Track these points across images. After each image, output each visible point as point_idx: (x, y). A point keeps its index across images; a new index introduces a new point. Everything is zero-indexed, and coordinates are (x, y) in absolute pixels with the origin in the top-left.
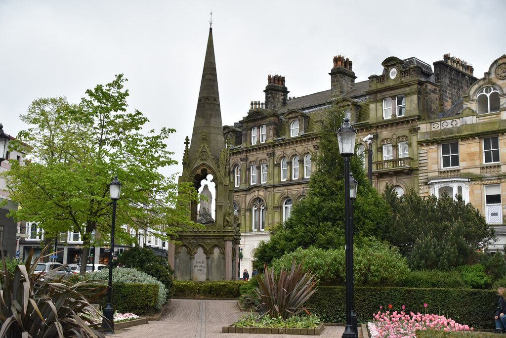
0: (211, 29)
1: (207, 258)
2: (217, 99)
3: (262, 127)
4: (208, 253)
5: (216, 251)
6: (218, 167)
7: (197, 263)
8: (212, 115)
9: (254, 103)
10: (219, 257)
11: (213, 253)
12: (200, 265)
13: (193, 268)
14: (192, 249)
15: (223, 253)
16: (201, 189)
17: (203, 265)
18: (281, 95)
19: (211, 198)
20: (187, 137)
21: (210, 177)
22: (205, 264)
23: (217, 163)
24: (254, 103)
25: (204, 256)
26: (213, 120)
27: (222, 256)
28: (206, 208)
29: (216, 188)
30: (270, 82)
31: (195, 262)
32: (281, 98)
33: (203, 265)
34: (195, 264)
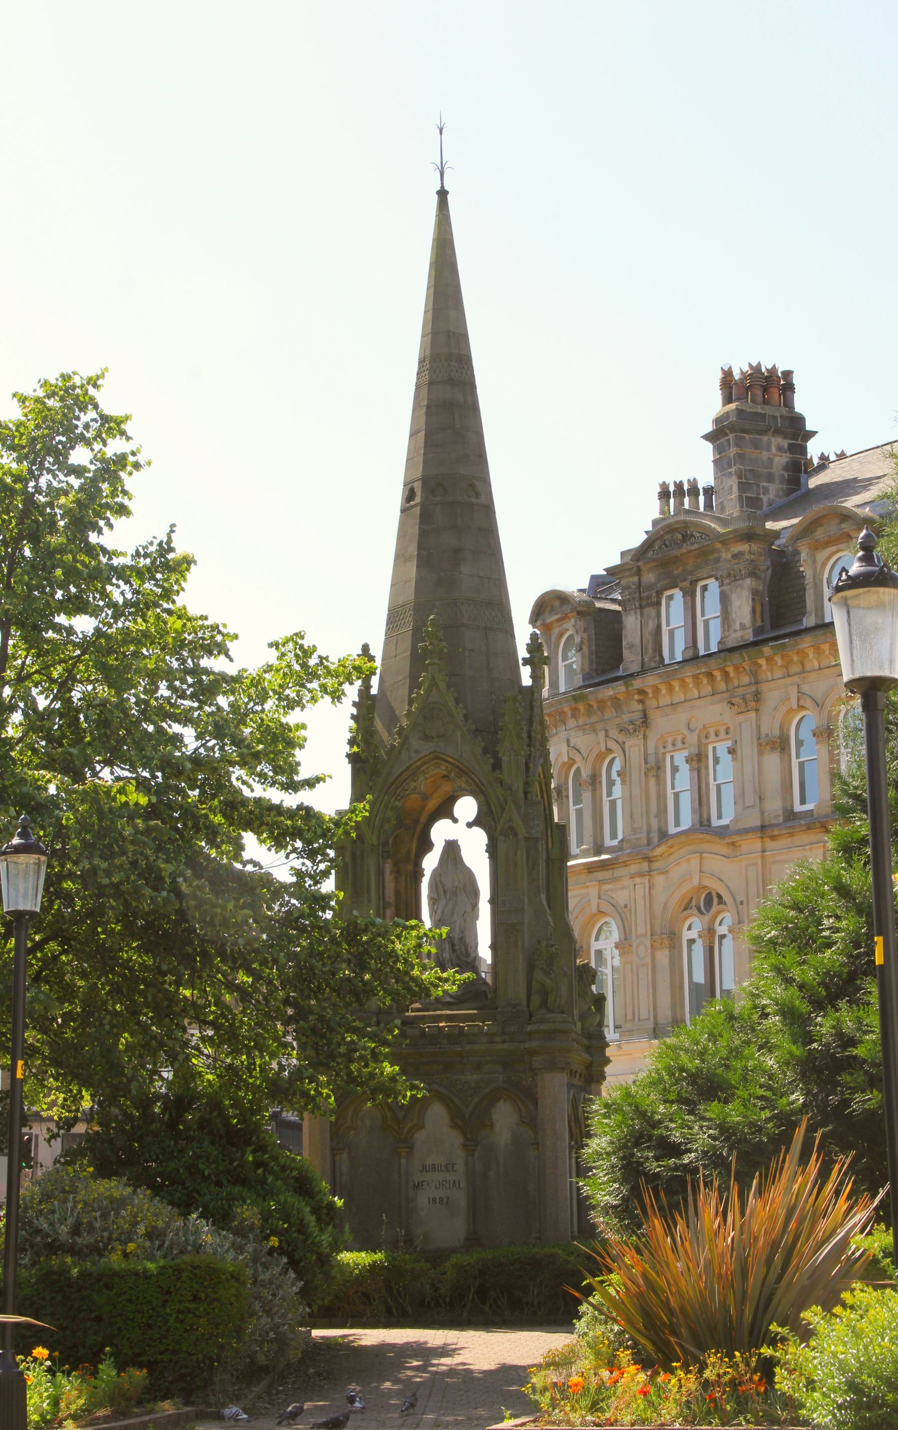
0: (443, 194)
1: (469, 1145)
2: (479, 486)
3: (705, 588)
4: (471, 1124)
5: (504, 1118)
6: (497, 766)
7: (424, 1169)
8: (457, 551)
9: (672, 488)
11: (492, 1126)
15: (531, 1120)
16: (430, 862)
17: (450, 1177)
18: (780, 449)
19: (476, 893)
20: (366, 648)
21: (467, 807)
23: (491, 750)
24: (672, 488)
25: (455, 1139)
26: (466, 569)
29: (492, 849)
30: (728, 400)
32: (781, 460)
33: (450, 1177)
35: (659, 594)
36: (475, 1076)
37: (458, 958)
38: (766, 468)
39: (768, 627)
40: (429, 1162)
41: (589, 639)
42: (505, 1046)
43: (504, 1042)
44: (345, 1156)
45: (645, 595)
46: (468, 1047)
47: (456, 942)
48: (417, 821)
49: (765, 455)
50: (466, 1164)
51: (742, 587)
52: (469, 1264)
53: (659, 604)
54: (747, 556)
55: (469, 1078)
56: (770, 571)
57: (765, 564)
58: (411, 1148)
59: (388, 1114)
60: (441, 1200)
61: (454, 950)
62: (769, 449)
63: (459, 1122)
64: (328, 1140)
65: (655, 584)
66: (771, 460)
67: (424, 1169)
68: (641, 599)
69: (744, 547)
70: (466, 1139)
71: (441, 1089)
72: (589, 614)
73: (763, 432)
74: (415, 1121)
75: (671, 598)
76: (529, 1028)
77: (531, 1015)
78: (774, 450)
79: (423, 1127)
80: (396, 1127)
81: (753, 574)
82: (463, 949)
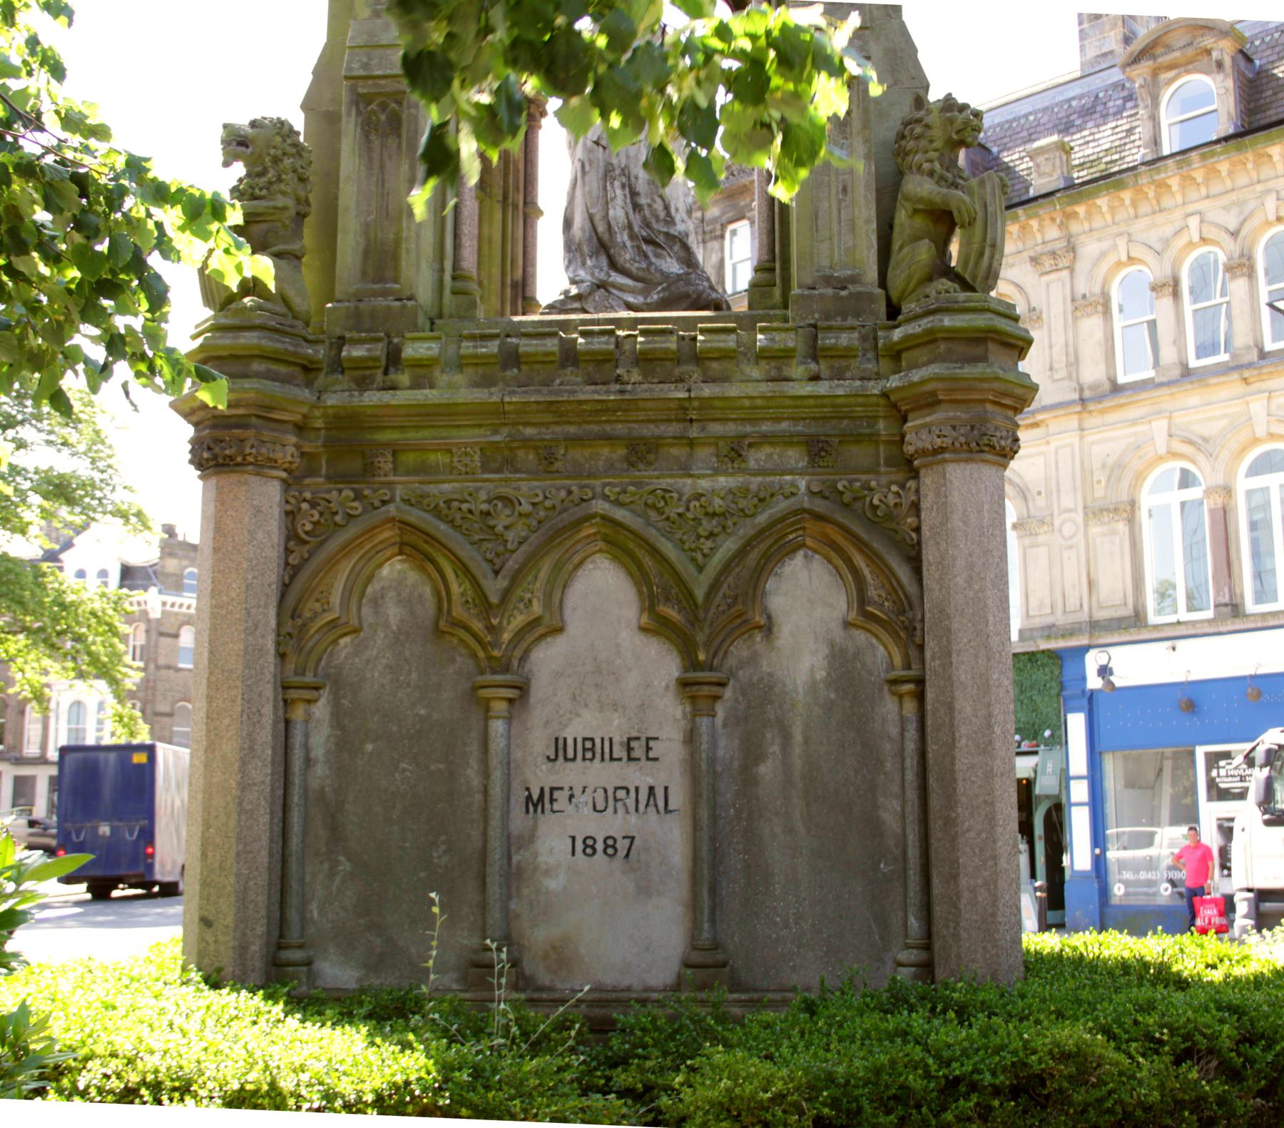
1: (698, 687)
4: (705, 623)
5: (807, 607)
7: (560, 751)
10: (843, 667)
11: (768, 629)
12: (600, 774)
13: (519, 821)
14: (494, 587)
17: (638, 776)
22: (668, 771)
25: (663, 665)
27: (880, 654)
31: (539, 742)
33: (638, 776)
34: (540, 776)
35: (723, 227)
36: (722, 480)
37: (647, 225)
40: (574, 731)
42: (822, 388)
43: (815, 378)
44: (321, 710)
45: (707, 229)
46: (707, 391)
50: (691, 738)
52: (779, 1098)
53: (722, 237)
55: (704, 484)
58: (523, 689)
59: (456, 588)
60: (610, 845)
61: (637, 207)
63: (672, 613)
64: (271, 658)
65: (720, 217)
67: (560, 751)
68: (704, 233)
70: (691, 663)
71: (620, 514)
74: (537, 608)
75: (734, 233)
76: (897, 334)
77: (893, 312)
79: (559, 630)
80: (478, 626)
82: (659, 206)
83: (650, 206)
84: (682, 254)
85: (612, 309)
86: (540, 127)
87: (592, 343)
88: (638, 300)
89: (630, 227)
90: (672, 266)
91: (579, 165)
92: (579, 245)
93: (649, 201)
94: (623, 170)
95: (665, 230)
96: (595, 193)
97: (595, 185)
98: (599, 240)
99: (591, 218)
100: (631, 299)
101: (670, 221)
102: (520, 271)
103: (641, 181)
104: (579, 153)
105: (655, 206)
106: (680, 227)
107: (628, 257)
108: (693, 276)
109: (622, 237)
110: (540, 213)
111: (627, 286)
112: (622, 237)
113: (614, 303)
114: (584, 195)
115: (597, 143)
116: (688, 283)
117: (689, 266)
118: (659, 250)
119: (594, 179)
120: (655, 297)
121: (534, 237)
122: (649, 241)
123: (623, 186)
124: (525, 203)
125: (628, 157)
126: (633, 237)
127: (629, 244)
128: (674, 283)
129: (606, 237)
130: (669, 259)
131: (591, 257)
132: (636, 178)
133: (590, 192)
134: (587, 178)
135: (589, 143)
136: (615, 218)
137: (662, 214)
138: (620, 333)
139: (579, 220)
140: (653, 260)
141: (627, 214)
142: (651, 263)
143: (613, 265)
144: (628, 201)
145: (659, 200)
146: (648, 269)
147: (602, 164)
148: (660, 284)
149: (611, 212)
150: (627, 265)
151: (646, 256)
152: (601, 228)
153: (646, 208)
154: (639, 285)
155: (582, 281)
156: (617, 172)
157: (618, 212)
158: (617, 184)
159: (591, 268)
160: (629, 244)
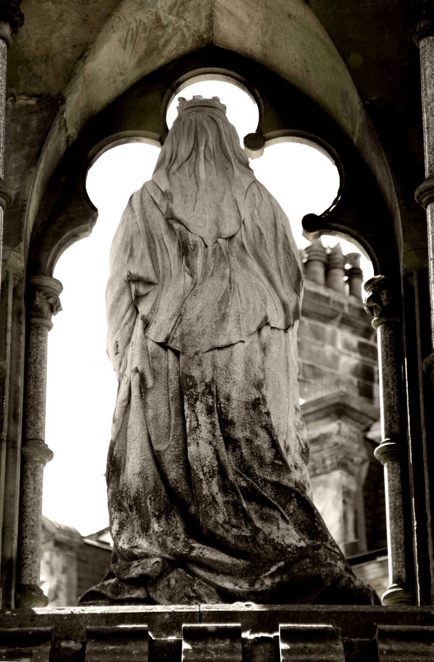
18: (347, 346)
28: (236, 391)
37: (244, 469)
38: (330, 366)
39: (363, 546)
41: (69, 585)
47: (236, 412)
48: (53, 104)
49: (328, 349)
51: (326, 484)
54: (336, 439)
56: (365, 467)
57: (359, 455)
61: (231, 442)
62: (333, 343)
66: (336, 358)
69: (330, 427)
72: (71, 548)
73: (327, 319)
78: (340, 346)
81: (342, 465)
83: (249, 441)
84: (301, 516)
85: (200, 599)
86: (49, 327)
87: (205, 651)
88: (244, 586)
89: (222, 471)
90: (290, 536)
91: (135, 380)
92: (136, 499)
93: (248, 434)
94: (208, 386)
95: (274, 479)
96: (163, 420)
97: (163, 409)
98: (171, 491)
99: (157, 458)
100: (229, 585)
101: (280, 464)
102: (15, 545)
103: (234, 404)
104: (134, 358)
105: (257, 442)
106: (296, 475)
107: (221, 518)
108: (321, 551)
109: (211, 488)
110: (49, 454)
111: (222, 564)
112: (211, 488)
113: (202, 591)
114: (146, 423)
115: (164, 345)
116: (317, 562)
117: (311, 537)
118: (267, 510)
119: (159, 399)
120: (268, 582)
121: (38, 492)
122: (252, 495)
123: (210, 411)
124: (25, 441)
125: (215, 368)
126: (226, 487)
127: (220, 498)
128: (297, 560)
129: (182, 487)
130: (282, 525)
131: (158, 518)
132: (228, 399)
133: (156, 418)
134: (150, 398)
135: (151, 345)
136: (198, 459)
137: (269, 455)
138: (247, 635)
139: (135, 462)
140: (258, 524)
141: (216, 452)
142: (256, 530)
143: (197, 531)
144: (218, 433)
145: (263, 434)
146: (253, 538)
147: (173, 376)
148: (274, 563)
149: (192, 449)
150: (220, 531)
151: (248, 520)
152: (174, 473)
153: (243, 445)
154: (241, 563)
155: (146, 556)
156: (200, 389)
157: (201, 450)
158: (199, 406)
159: (159, 535)
160: (220, 498)
